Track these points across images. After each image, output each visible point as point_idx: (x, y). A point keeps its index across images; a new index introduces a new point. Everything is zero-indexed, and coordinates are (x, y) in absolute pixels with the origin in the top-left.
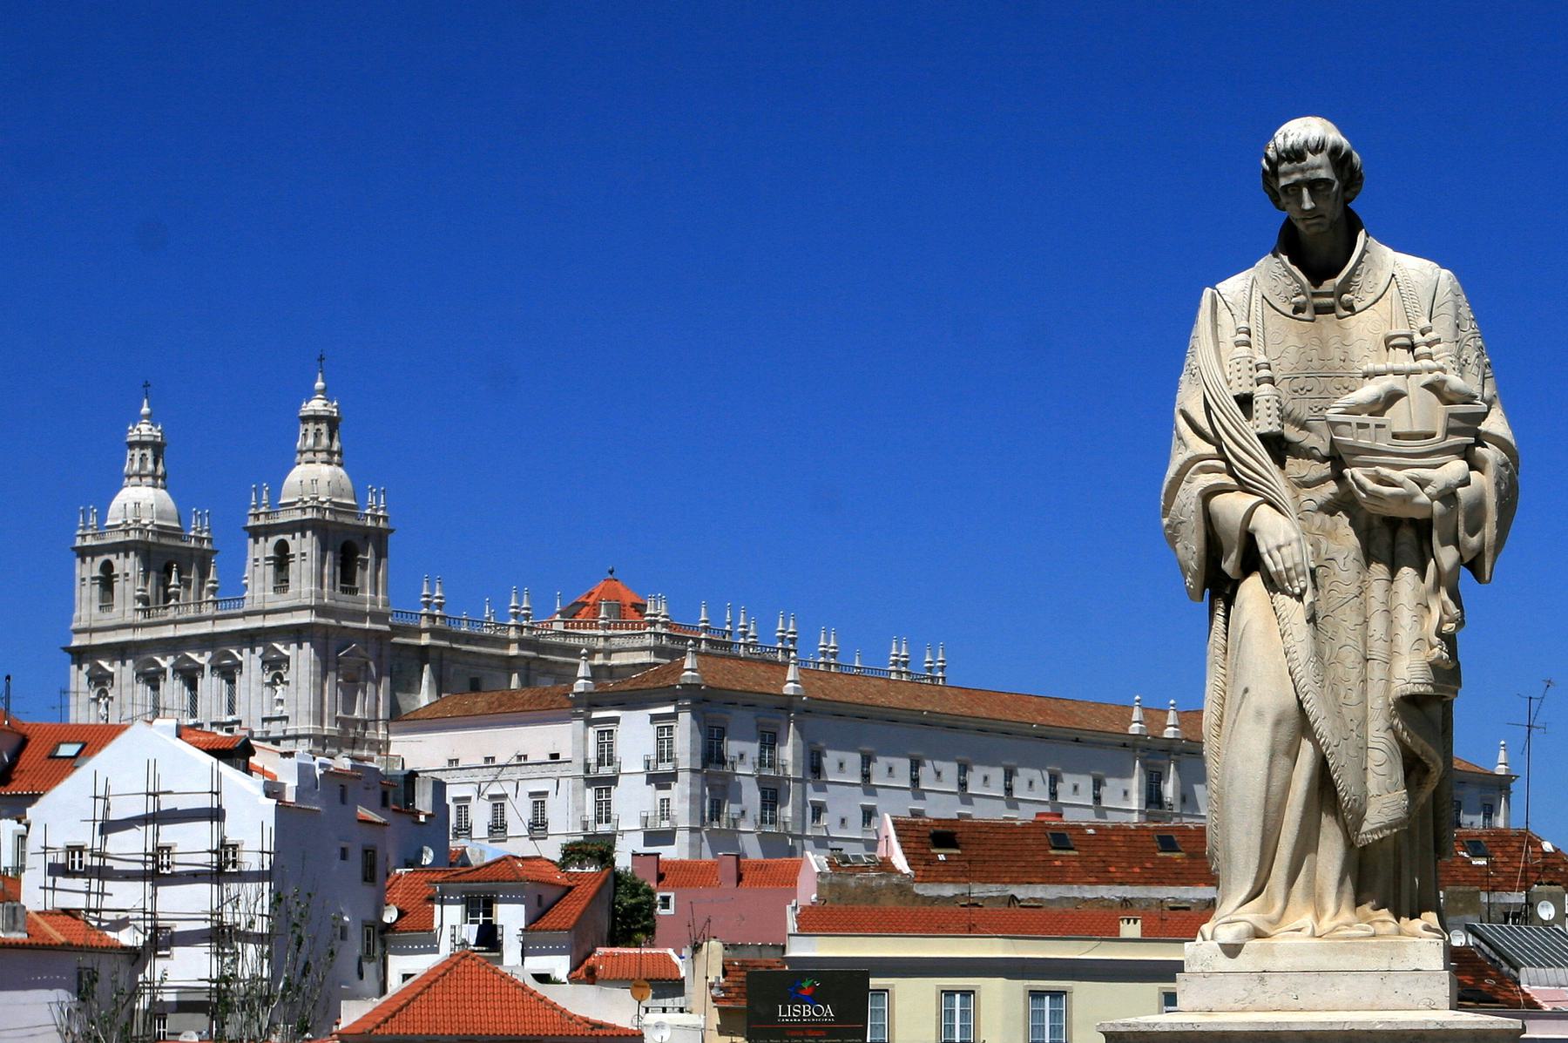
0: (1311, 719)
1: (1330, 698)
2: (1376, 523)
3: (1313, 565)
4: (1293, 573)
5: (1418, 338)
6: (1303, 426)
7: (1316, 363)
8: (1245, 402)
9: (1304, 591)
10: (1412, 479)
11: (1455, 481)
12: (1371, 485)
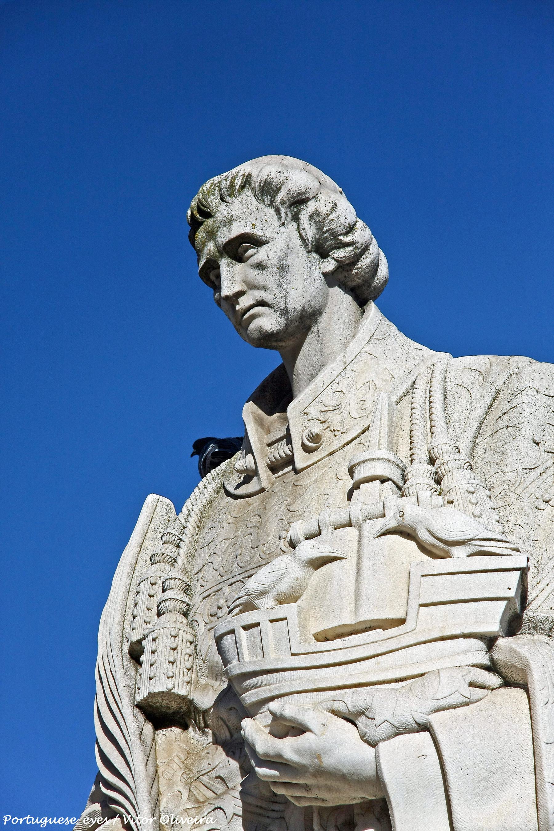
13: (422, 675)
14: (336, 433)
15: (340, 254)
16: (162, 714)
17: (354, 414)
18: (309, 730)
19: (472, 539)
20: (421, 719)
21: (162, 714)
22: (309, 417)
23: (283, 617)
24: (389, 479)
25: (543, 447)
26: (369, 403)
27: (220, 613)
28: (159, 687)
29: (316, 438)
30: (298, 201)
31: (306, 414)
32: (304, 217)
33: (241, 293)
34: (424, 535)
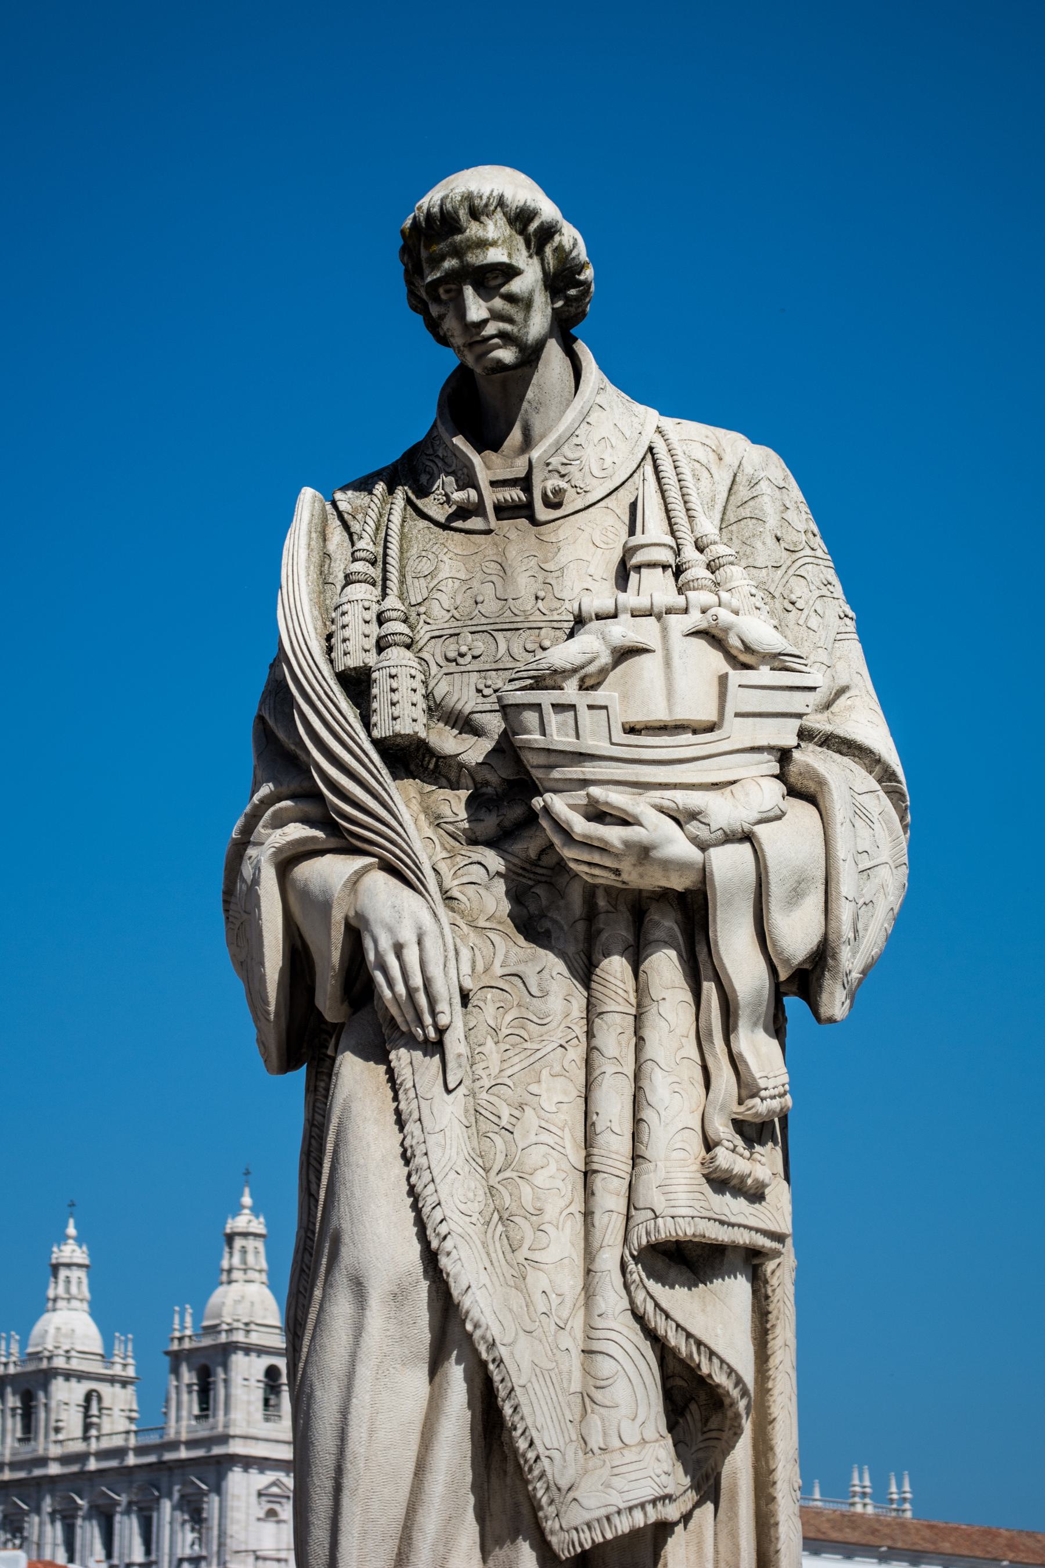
0: (455, 1292)
1: (497, 1248)
2: (602, 903)
3: (468, 984)
4: (422, 1000)
5: (689, 553)
6: (466, 725)
7: (491, 606)
8: (357, 684)
9: (441, 1031)
10: (661, 810)
11: (755, 816)
12: (580, 825)
13: (735, 782)
14: (579, 490)
15: (573, 292)
16: (406, 758)
17: (596, 473)
18: (641, 825)
19: (780, 654)
20: (747, 827)
21: (406, 758)
22: (550, 468)
23: (603, 704)
24: (670, 566)
25: (783, 544)
26: (608, 463)
27: (460, 660)
28: (405, 727)
29: (559, 492)
30: (548, 232)
31: (548, 464)
32: (548, 250)
33: (484, 322)
34: (734, 641)
